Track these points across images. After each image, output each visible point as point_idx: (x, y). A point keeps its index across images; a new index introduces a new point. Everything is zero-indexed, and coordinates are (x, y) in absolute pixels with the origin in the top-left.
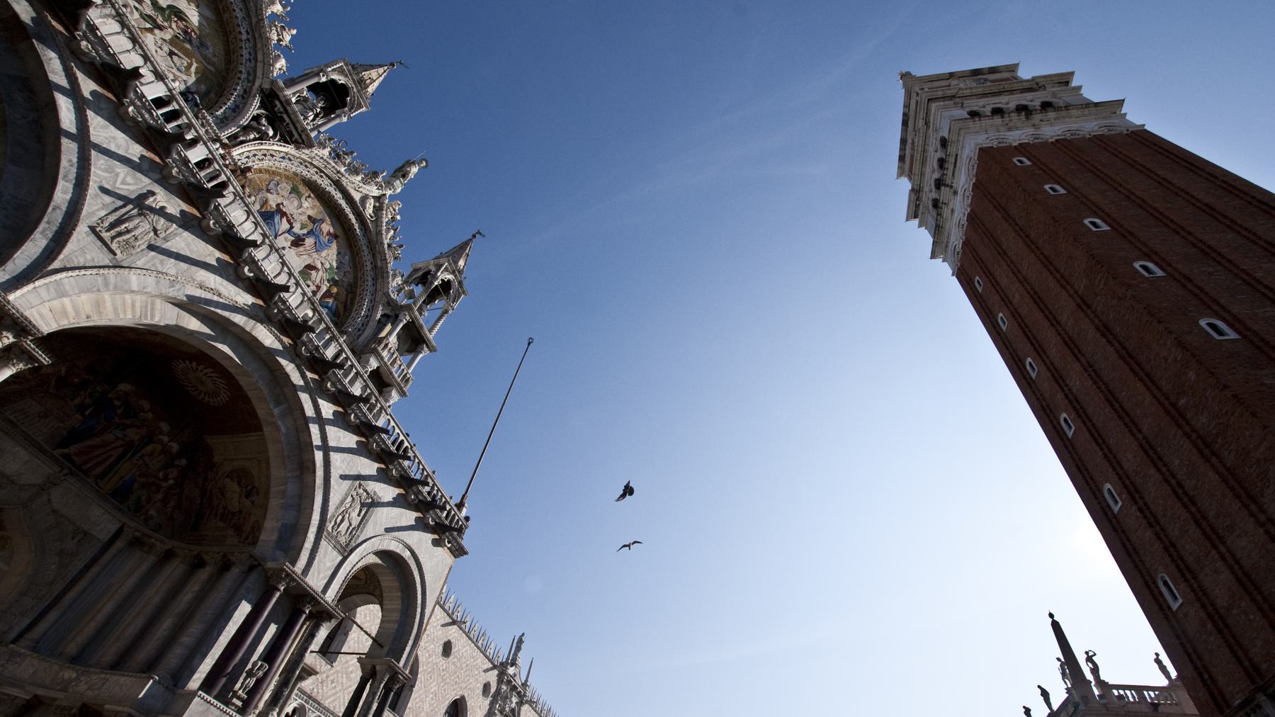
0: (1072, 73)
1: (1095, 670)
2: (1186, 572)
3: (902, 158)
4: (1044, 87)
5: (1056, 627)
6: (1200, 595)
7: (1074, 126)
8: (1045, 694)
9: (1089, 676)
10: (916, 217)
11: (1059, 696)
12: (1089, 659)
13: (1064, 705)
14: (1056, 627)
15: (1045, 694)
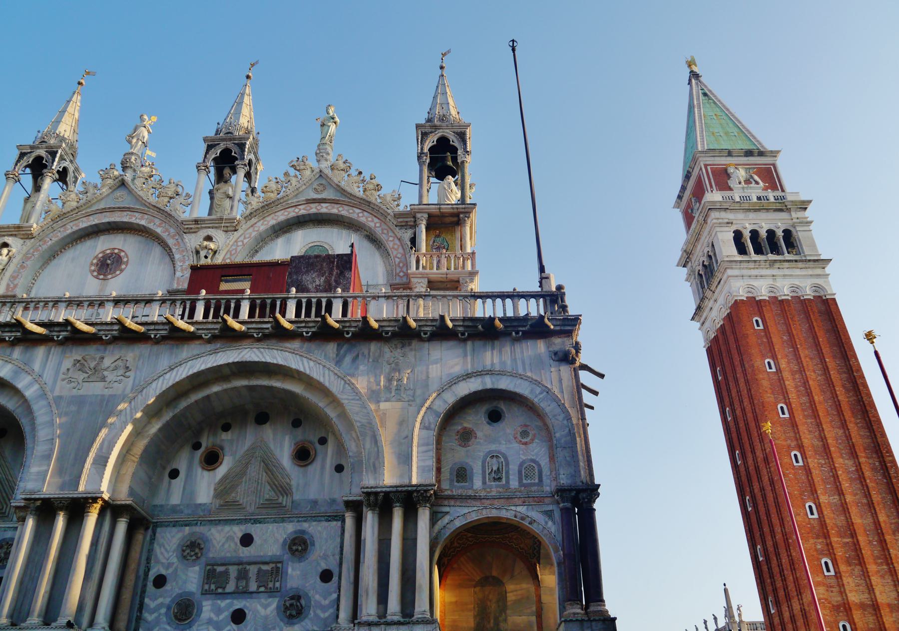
0: (810, 201)
1: (740, 615)
2: (777, 603)
3: (680, 197)
4: (789, 210)
5: (726, 591)
6: (780, 613)
7: (797, 282)
8: (715, 619)
9: (737, 619)
10: (684, 266)
11: (722, 623)
12: (739, 609)
13: (724, 627)
14: (726, 591)
15: (715, 619)
